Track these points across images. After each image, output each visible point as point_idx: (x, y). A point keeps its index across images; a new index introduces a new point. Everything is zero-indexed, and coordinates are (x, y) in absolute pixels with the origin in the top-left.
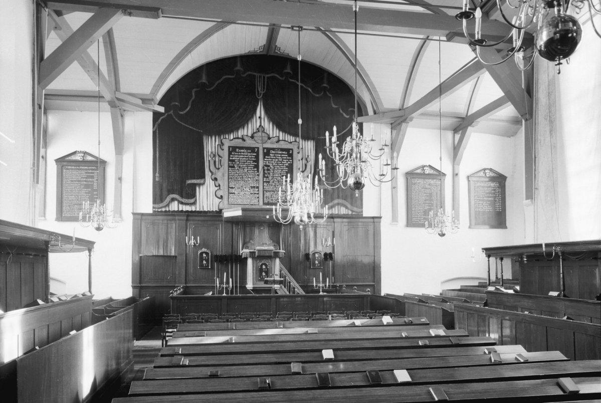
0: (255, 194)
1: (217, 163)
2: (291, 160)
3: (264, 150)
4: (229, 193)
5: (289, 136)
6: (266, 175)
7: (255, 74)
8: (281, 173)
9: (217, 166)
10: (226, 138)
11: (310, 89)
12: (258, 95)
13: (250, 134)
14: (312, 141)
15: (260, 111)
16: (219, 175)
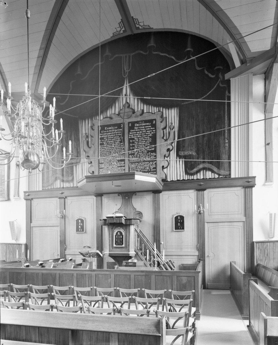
0: (121, 166)
1: (90, 143)
2: (155, 130)
3: (129, 124)
4: (99, 168)
5: (153, 107)
6: (131, 148)
7: (121, 55)
8: (145, 144)
9: (90, 146)
10: (97, 119)
11: (173, 57)
12: (124, 74)
13: (117, 113)
14: (176, 109)
15: (126, 88)
16: (91, 153)
